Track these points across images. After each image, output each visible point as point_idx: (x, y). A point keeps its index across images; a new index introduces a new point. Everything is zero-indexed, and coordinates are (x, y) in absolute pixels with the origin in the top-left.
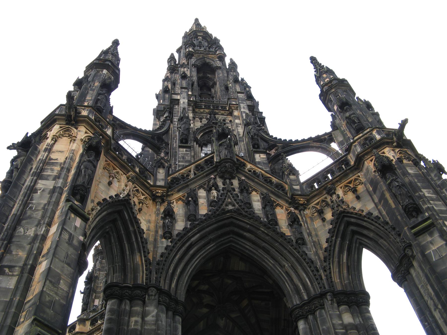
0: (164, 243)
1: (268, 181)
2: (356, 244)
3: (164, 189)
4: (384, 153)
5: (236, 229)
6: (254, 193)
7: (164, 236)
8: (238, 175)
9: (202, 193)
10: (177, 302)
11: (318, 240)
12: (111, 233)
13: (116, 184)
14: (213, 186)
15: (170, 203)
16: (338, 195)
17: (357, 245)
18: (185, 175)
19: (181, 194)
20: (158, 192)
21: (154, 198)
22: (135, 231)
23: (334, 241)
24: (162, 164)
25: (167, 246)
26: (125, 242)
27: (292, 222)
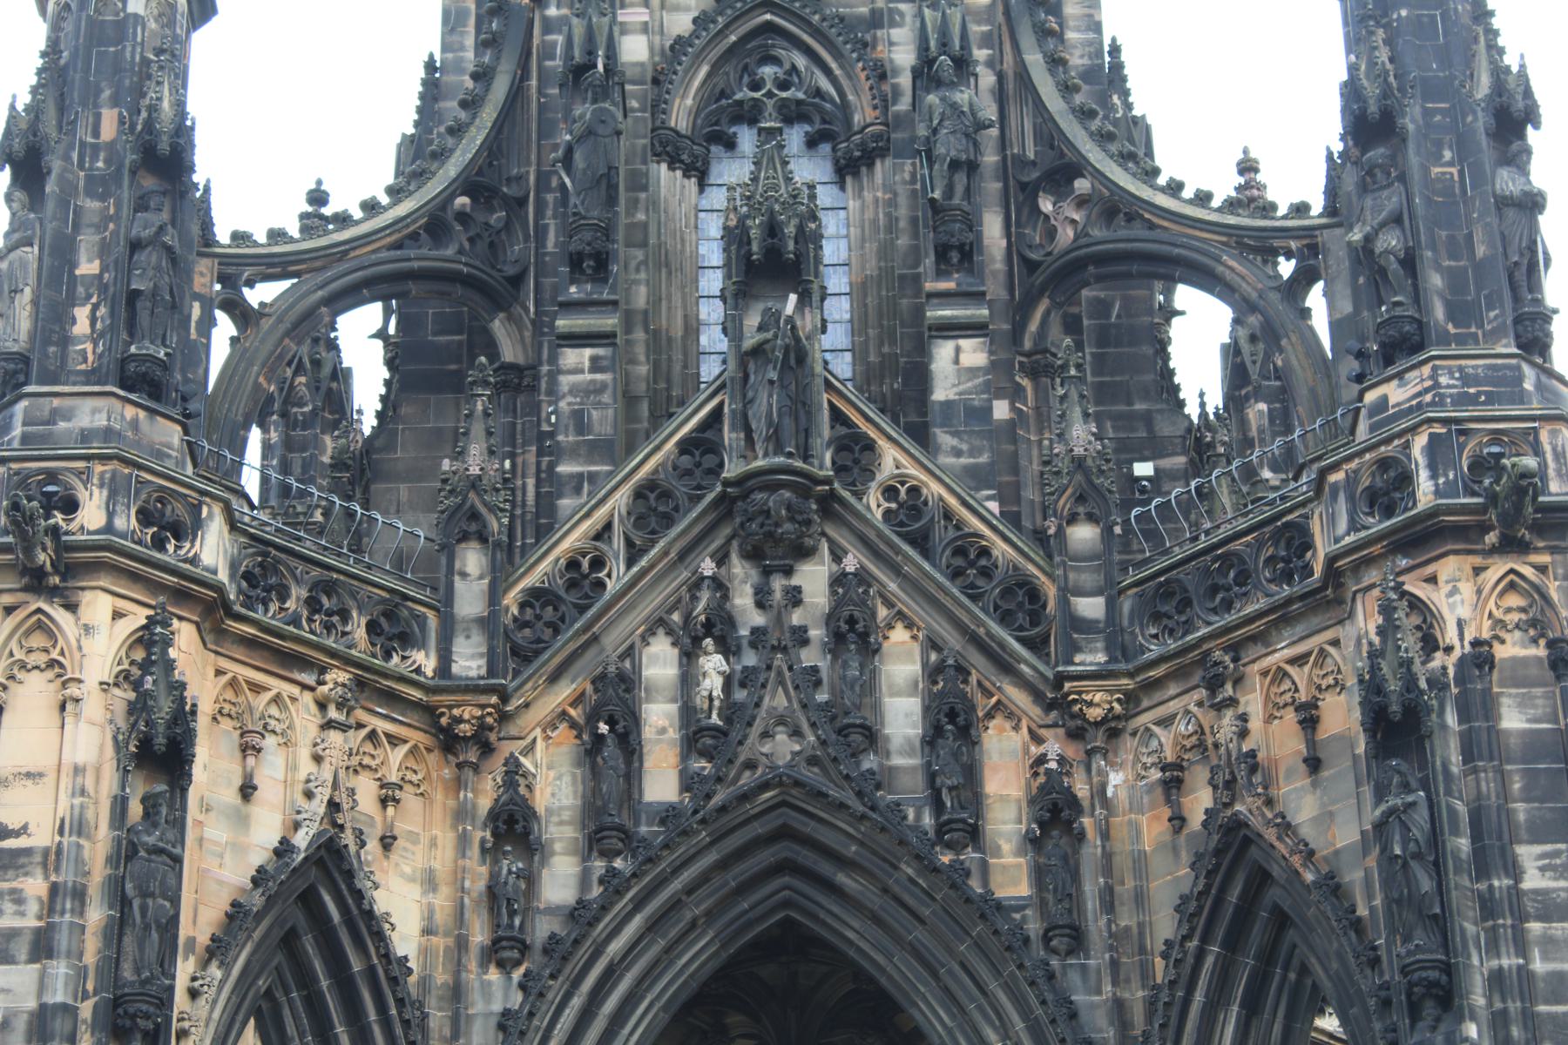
0: (495, 992)
1: (968, 558)
2: (1286, 968)
3: (483, 699)
4: (1432, 580)
5: (806, 857)
6: (899, 635)
8: (831, 531)
9: (660, 662)
11: (1141, 925)
12: (279, 995)
13: (272, 769)
14: (708, 627)
15: (513, 771)
16: (1244, 718)
17: (1292, 976)
18: (585, 563)
19: (564, 691)
20: (460, 720)
21: (448, 742)
22: (371, 971)
23: (1190, 960)
24: (474, 516)
25: (506, 1013)
26: (339, 1029)
27: (1041, 825)
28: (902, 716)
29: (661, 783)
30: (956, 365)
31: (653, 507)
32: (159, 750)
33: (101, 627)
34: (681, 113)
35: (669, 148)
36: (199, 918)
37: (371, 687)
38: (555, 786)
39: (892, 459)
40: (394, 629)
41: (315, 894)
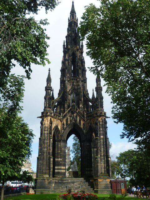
7: (63, 129)
9: (69, 118)
10: (65, 141)
13: (55, 123)
21: (61, 121)
28: (78, 120)
29: (69, 123)
30: (81, 105)
31: (69, 111)
32: (51, 123)
33: (49, 118)
34: (70, 93)
35: (69, 94)
36: (53, 129)
37: (58, 119)
38: (65, 123)
39: (78, 110)
40: (59, 117)
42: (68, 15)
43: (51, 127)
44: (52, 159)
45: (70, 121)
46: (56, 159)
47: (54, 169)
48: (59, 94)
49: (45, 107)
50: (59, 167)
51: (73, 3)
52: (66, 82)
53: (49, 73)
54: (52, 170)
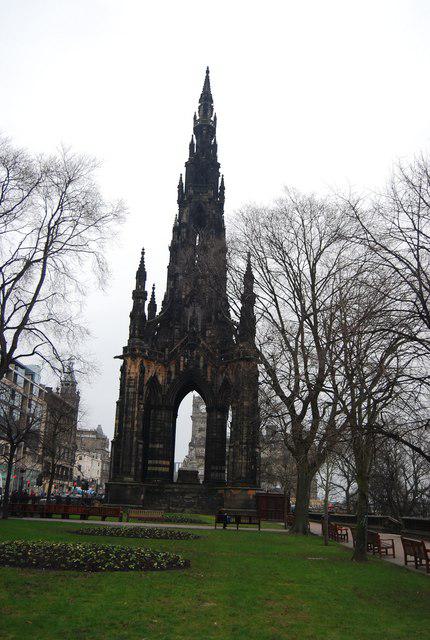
28: (201, 364)
36: (146, 382)
37: (159, 362)
38: (173, 369)
41: (154, 379)
42: (194, 106)
43: (142, 378)
44: (141, 446)
45: (184, 365)
46: (150, 446)
47: (145, 465)
48: (164, 303)
49: (131, 336)
50: (160, 462)
51: (208, 72)
52: (180, 277)
53: (143, 258)
54: (140, 467)
